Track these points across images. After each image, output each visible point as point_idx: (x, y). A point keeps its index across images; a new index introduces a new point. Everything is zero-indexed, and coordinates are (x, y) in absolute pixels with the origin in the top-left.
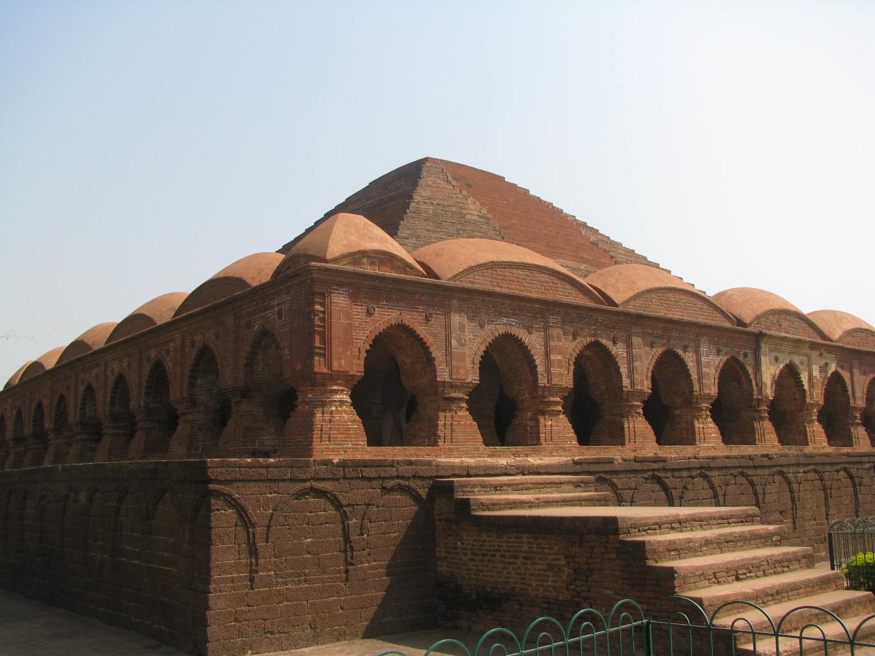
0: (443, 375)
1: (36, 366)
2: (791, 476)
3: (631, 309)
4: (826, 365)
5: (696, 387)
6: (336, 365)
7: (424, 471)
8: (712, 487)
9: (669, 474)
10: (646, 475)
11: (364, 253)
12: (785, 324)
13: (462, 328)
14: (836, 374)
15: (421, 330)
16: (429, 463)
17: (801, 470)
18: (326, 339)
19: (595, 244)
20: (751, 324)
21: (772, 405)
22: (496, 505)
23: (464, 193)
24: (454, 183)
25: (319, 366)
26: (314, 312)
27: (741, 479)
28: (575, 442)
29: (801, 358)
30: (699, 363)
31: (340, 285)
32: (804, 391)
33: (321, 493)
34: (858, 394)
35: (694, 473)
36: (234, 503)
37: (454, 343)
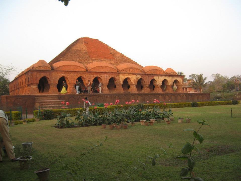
4: (138, 77)
9: (75, 96)
10: (70, 97)
11: (41, 66)
12: (131, 70)
14: (141, 79)
15: (48, 77)
17: (106, 96)
19: (111, 53)
20: (121, 71)
23: (85, 45)
24: (84, 43)
29: (131, 76)
31: (35, 72)
35: (81, 96)
37: (54, 78)
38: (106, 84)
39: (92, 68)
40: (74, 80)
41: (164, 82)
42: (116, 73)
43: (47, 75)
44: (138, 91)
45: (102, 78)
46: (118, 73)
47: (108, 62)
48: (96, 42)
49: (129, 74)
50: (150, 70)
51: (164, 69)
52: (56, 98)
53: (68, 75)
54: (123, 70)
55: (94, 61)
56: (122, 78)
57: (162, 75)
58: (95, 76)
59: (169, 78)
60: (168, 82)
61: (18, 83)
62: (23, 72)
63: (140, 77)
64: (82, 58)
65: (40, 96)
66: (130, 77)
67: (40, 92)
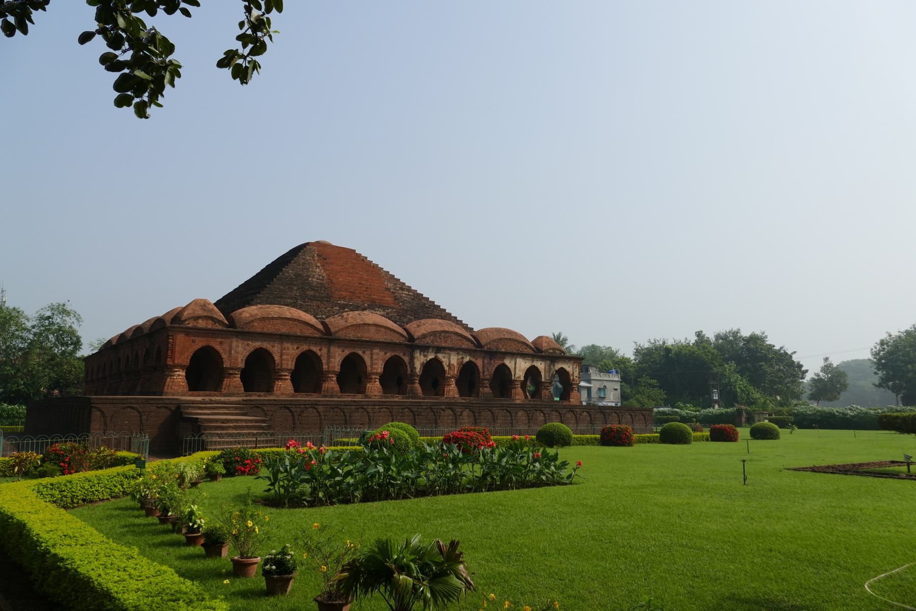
0: (226, 365)
1: (110, 341)
2: (370, 410)
3: (341, 335)
4: (463, 358)
5: (369, 369)
6: (176, 362)
7: (176, 402)
8: (318, 412)
11: (198, 318)
13: (237, 346)
14: (470, 362)
15: (218, 347)
16: (177, 399)
18: (173, 352)
19: (388, 289)
20: (418, 339)
21: (421, 376)
22: (195, 414)
25: (169, 362)
26: (168, 343)
27: (336, 410)
28: (292, 392)
30: (372, 358)
32: (445, 371)
33: (133, 408)
34: (486, 373)
36: (100, 410)
38: (376, 374)
39: (342, 329)
40: (288, 360)
41: (532, 373)
42: (406, 345)
43: (215, 344)
44: (461, 394)
45: (367, 359)
46: (412, 344)
47: (382, 313)
48: (349, 255)
49: (439, 349)
50: (494, 341)
51: (530, 337)
52: (241, 409)
53: (273, 347)
54: (424, 336)
55: (343, 307)
56: (420, 360)
57: (523, 356)
58: (347, 352)
59: (543, 364)
60: (540, 372)
61: (119, 359)
62: (138, 329)
63: (467, 359)
64: (313, 298)
65: (193, 402)
66: (440, 356)
67: (190, 390)
